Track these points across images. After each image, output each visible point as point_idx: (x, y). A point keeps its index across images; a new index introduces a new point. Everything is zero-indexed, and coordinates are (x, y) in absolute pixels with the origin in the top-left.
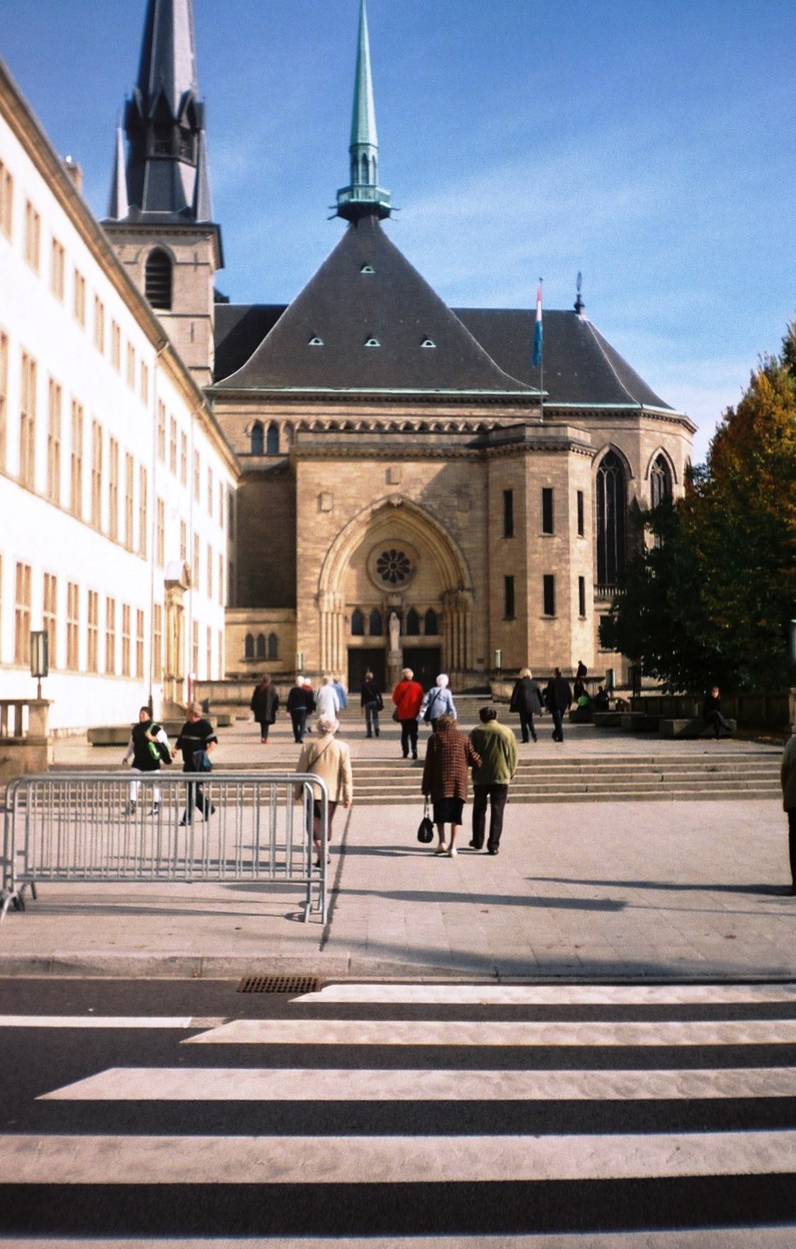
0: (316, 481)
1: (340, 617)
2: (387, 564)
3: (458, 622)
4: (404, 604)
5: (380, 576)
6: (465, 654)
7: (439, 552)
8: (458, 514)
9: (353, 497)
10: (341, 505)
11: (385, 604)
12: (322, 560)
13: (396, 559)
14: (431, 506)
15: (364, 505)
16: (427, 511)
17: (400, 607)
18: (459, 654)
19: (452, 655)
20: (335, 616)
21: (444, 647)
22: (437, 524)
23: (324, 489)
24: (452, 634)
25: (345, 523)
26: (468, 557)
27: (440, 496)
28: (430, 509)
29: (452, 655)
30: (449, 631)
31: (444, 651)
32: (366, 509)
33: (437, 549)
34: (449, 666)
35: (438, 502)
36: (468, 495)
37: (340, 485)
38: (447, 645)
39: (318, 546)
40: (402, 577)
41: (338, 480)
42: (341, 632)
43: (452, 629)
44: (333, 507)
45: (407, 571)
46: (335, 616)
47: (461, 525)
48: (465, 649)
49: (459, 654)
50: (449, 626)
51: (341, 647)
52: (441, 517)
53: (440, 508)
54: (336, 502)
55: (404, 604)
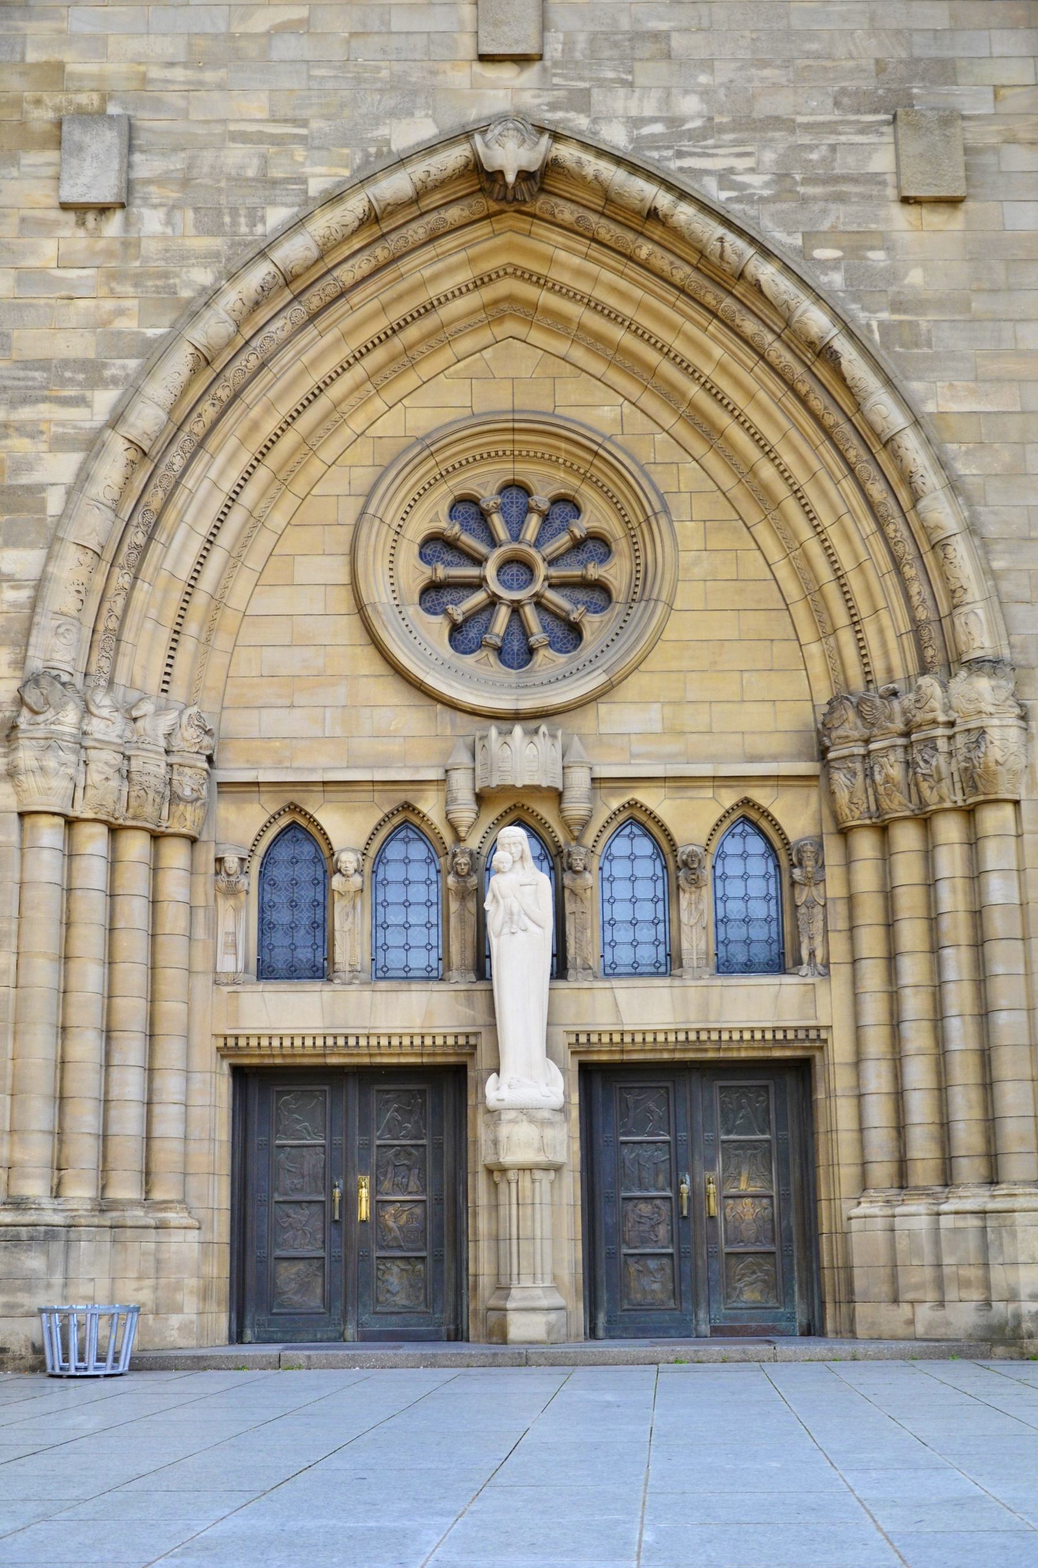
0: (32, 57)
1: (175, 854)
2: (479, 561)
3: (931, 884)
4: (579, 781)
5: (437, 627)
6: (988, 1085)
7: (783, 472)
8: (900, 218)
9: (259, 138)
10: (186, 182)
11: (462, 786)
12: (54, 502)
13: (533, 522)
14: (725, 178)
15: (316, 187)
16: (705, 208)
17: (558, 796)
18: (942, 1089)
19: (899, 1096)
20: (135, 846)
21: (840, 1048)
22: (767, 273)
23: (87, 99)
24: (892, 958)
25: (204, 277)
26: (962, 468)
27: (788, 125)
28: (718, 195)
29: (899, 1096)
30: (871, 942)
31: (841, 1080)
32: (334, 198)
33: (769, 453)
34: (882, 1172)
35: (769, 157)
36: (949, 118)
37: (179, 74)
38: (858, 1029)
39: (25, 413)
40: (574, 632)
41: (169, 47)
42: (173, 952)
43: (890, 925)
44: (129, 186)
45: (600, 587)
46: (135, 846)
47: (915, 277)
48: (986, 1057)
49: (942, 1089)
50: (870, 911)
51: (170, 1052)
52: (797, 240)
53: (782, 177)
54: (145, 166)
55: (579, 781)
